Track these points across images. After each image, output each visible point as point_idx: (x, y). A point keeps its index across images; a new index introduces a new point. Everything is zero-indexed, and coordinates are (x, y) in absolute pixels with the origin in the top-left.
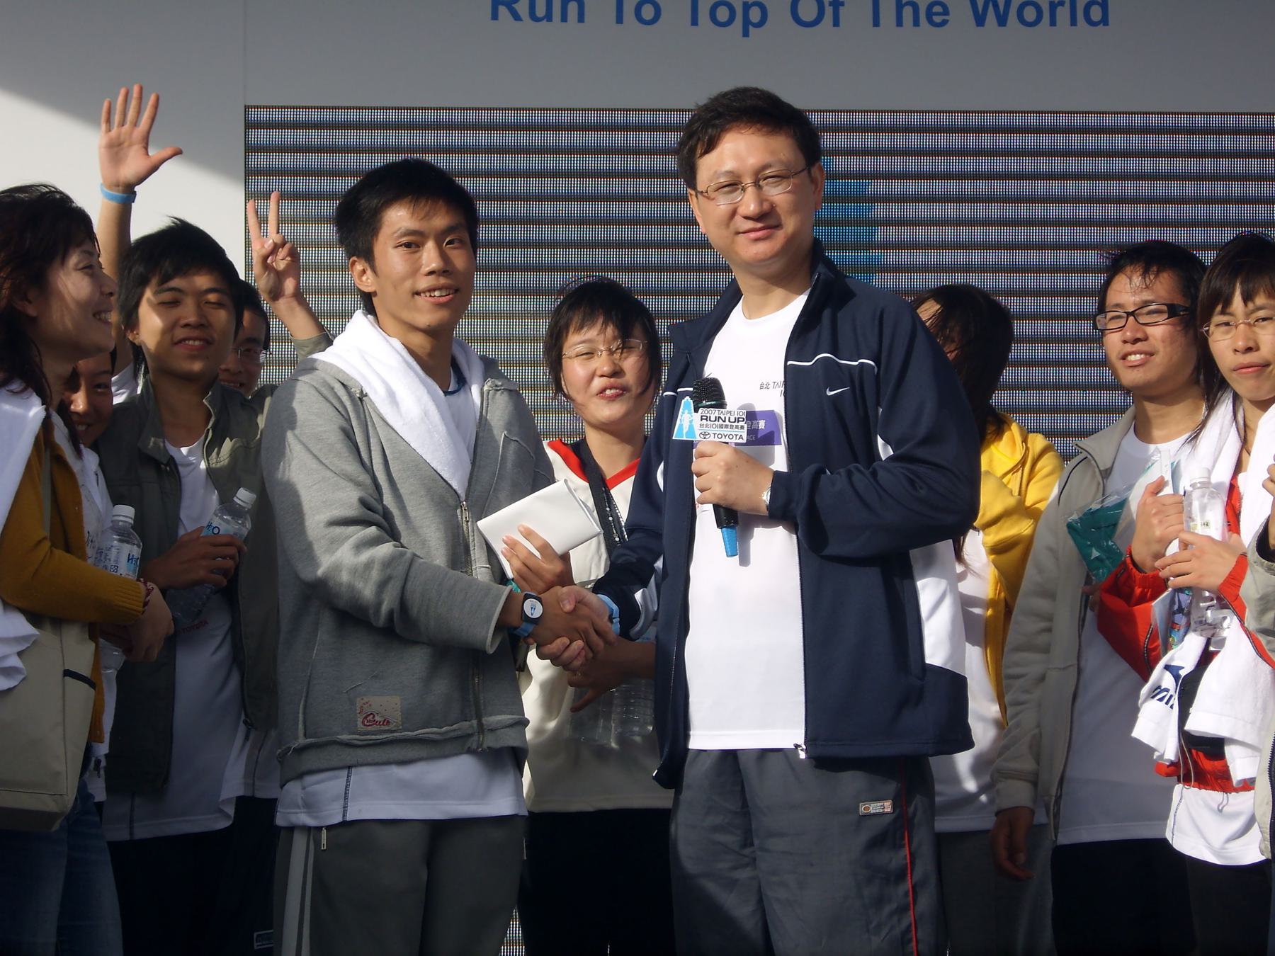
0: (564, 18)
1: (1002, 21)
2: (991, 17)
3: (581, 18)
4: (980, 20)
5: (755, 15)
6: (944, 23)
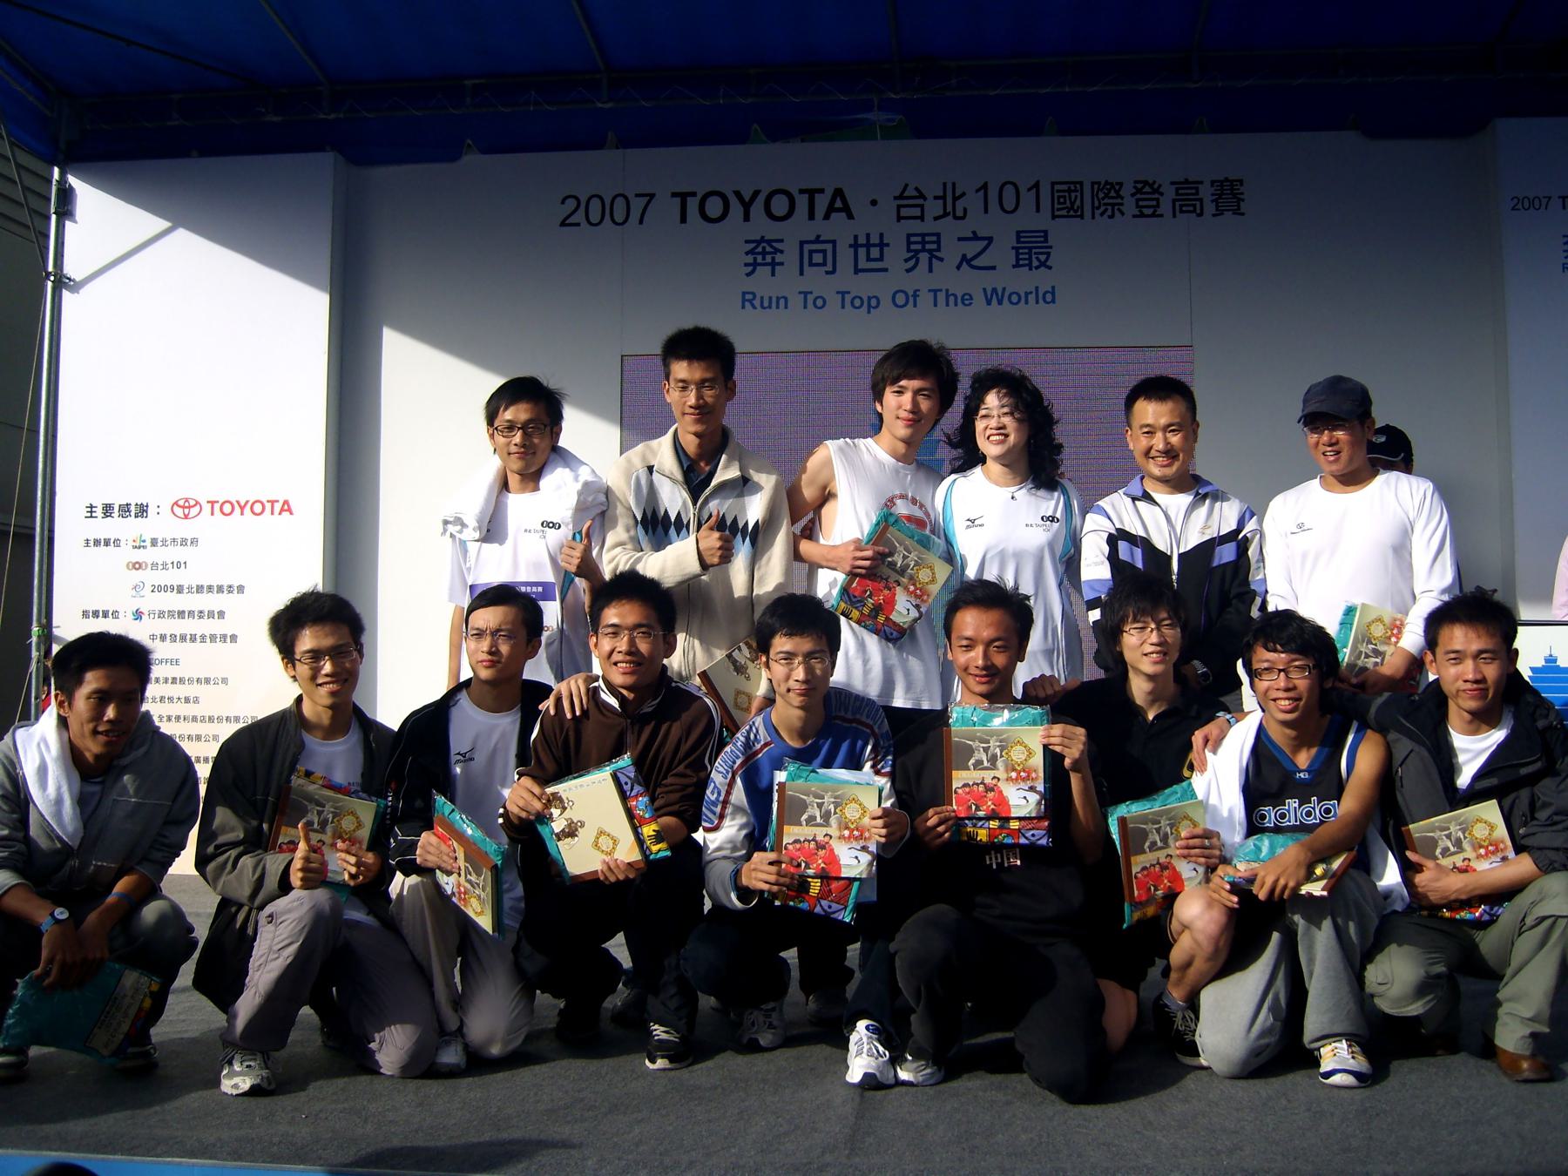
1: (1000, 302)
2: (994, 301)
4: (989, 303)
5: (874, 302)
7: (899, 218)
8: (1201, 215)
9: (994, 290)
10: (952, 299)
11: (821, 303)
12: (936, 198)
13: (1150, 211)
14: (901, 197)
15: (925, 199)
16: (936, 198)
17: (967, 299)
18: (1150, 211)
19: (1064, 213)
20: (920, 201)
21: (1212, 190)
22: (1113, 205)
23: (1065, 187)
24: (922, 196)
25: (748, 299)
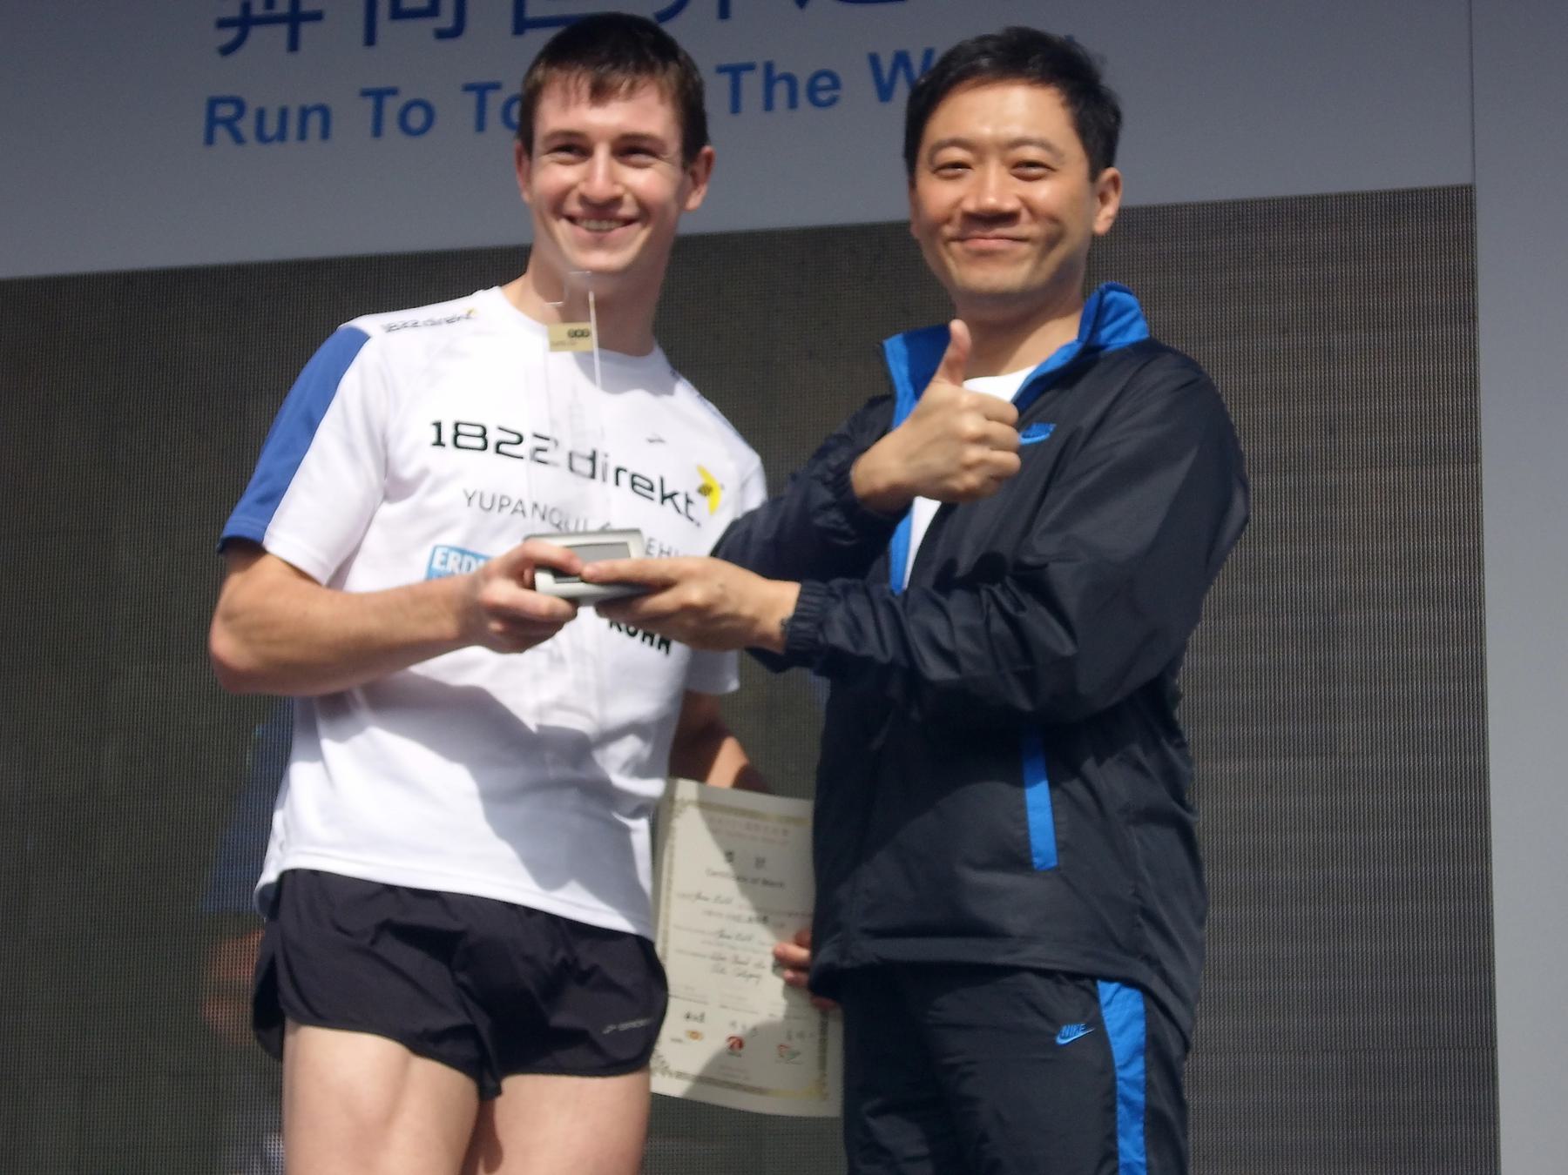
0: (302, 136)
3: (325, 134)
6: (832, 101)
9: (902, 59)
10: (781, 90)
11: (419, 118)
17: (822, 89)
25: (223, 118)
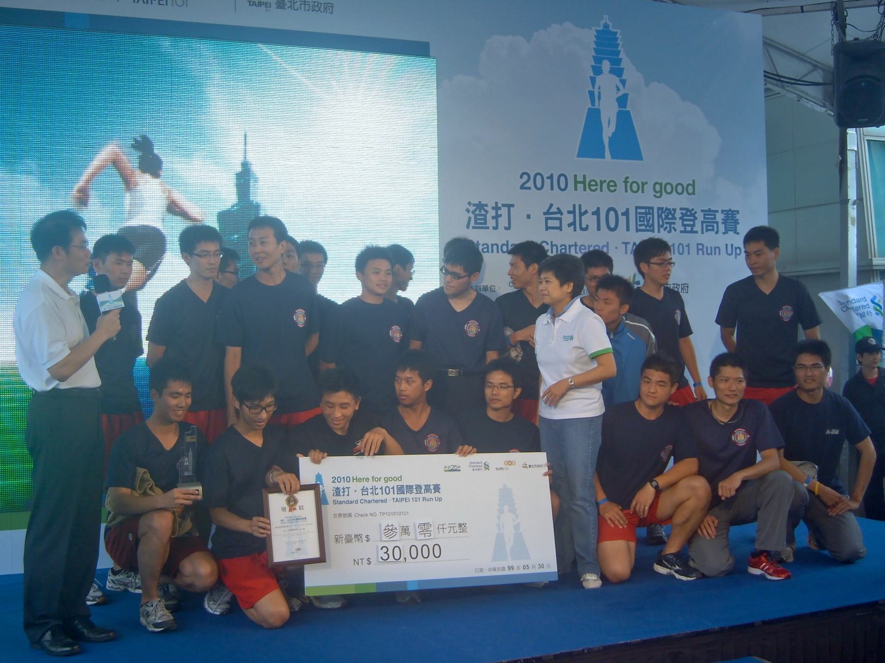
7: (547, 228)
8: (717, 233)
12: (569, 212)
13: (689, 229)
14: (547, 212)
15: (562, 214)
16: (569, 212)
18: (689, 229)
19: (643, 228)
20: (559, 216)
21: (722, 216)
22: (670, 224)
23: (643, 211)
24: (559, 212)
